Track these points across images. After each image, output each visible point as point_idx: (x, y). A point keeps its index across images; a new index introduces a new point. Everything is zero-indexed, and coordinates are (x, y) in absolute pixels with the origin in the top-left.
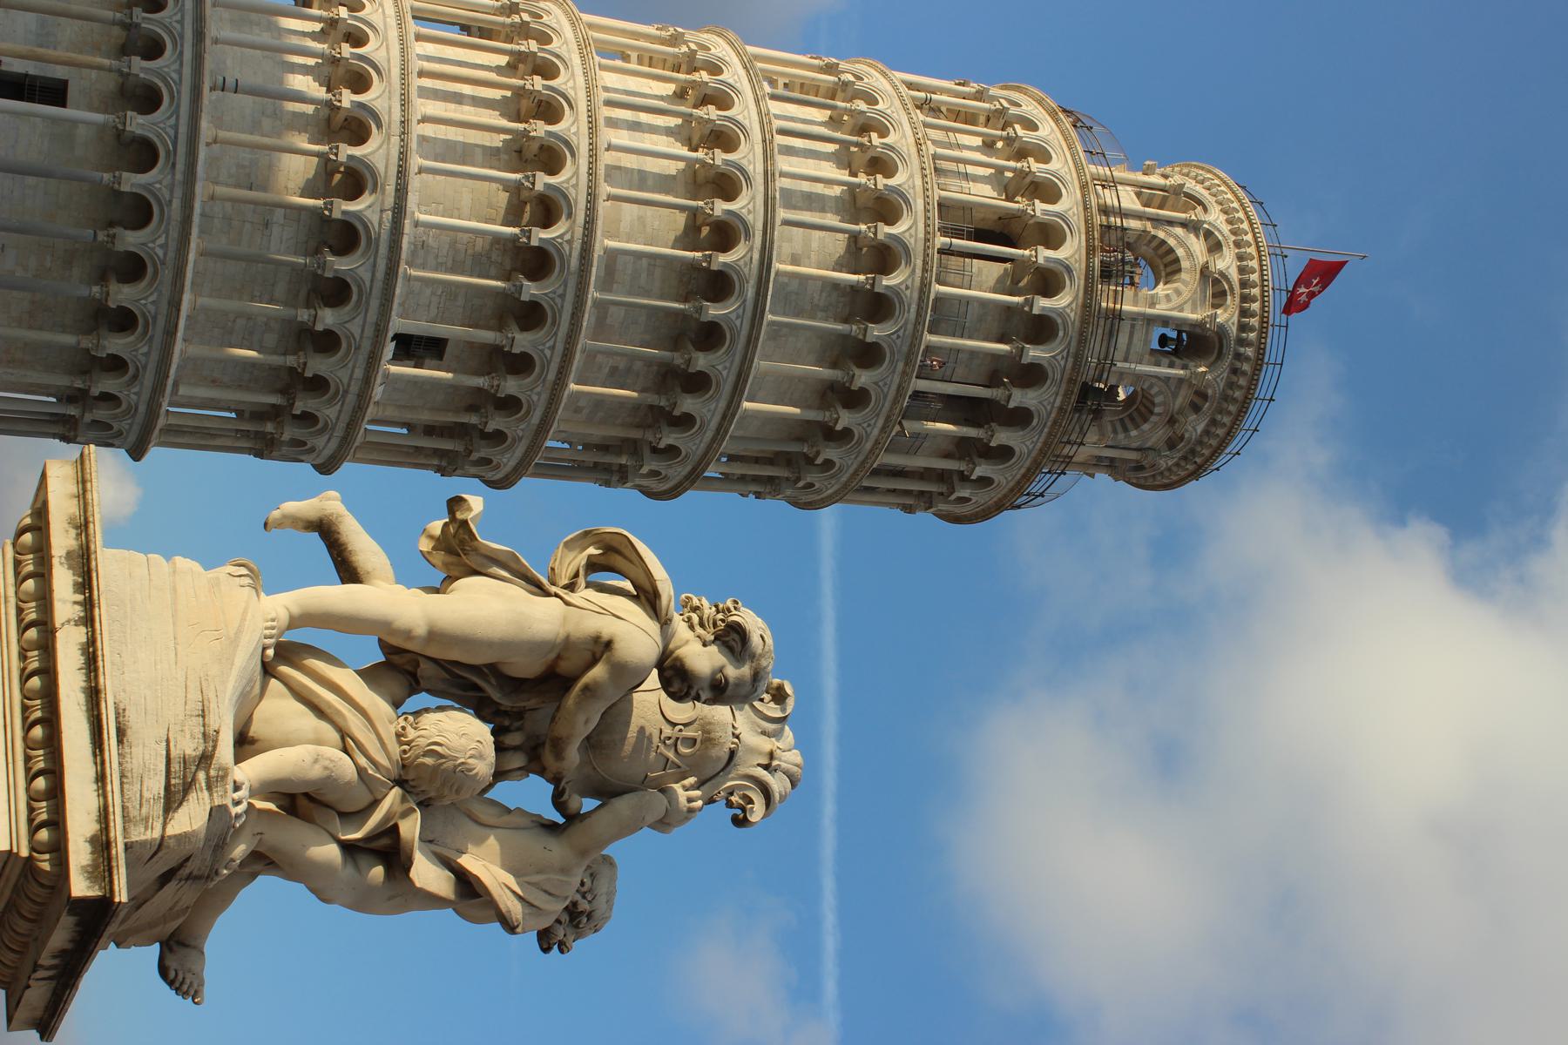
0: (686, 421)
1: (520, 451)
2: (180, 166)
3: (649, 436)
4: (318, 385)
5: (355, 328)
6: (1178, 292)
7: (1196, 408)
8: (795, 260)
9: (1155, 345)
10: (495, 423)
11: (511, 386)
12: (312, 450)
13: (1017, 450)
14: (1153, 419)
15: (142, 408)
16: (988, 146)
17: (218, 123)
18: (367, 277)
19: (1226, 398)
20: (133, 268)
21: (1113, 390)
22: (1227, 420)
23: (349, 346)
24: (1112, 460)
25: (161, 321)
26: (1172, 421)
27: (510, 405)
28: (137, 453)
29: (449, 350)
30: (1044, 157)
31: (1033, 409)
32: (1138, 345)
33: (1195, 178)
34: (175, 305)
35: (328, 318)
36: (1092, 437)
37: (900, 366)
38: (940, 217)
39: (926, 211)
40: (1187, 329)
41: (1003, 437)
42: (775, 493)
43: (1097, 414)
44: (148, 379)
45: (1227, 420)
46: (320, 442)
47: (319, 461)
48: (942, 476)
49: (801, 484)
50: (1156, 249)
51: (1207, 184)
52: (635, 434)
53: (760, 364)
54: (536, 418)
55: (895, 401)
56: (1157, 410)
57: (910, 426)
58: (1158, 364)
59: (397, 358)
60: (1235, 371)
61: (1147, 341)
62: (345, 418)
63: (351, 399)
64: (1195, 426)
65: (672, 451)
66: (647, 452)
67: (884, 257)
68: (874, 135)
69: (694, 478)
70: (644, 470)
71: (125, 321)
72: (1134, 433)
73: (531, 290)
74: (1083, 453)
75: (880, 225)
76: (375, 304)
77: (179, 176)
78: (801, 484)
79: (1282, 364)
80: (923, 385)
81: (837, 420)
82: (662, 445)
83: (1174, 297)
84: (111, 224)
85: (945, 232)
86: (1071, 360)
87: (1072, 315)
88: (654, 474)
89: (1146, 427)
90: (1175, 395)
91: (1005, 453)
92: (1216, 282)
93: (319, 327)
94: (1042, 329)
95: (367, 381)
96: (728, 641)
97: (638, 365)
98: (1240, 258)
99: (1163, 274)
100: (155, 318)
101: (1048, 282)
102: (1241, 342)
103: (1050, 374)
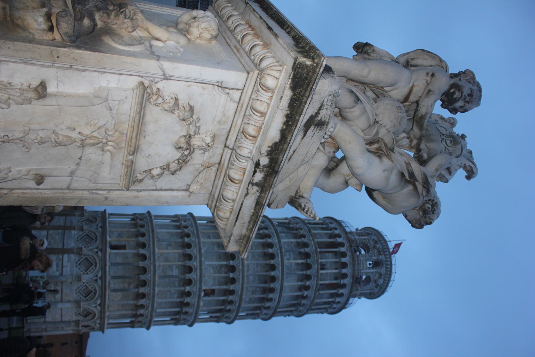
0: (270, 300)
1: (235, 313)
2: (152, 259)
3: (263, 304)
4: (188, 304)
5: (194, 289)
6: (371, 253)
7: (380, 278)
8: (288, 259)
9: (368, 266)
10: (228, 307)
11: (231, 298)
12: (188, 321)
13: (345, 294)
14: (372, 282)
15: (149, 316)
16: (323, 229)
17: (159, 249)
18: (195, 277)
19: (386, 273)
20: (144, 284)
21: (361, 277)
22: (387, 279)
23: (194, 294)
24: (364, 293)
25: (151, 294)
26: (375, 282)
27: (231, 302)
28: (148, 328)
29: (216, 292)
30: (336, 229)
31: (346, 283)
32: (365, 266)
33: (367, 230)
34: (154, 290)
35: (188, 288)
36: (360, 288)
37: (316, 279)
38: (318, 245)
39: (314, 244)
40: (374, 260)
41: (341, 291)
42: (292, 315)
43: (359, 283)
44: (150, 309)
45: (387, 279)
46: (190, 318)
47: (189, 324)
48: (329, 303)
49: (298, 311)
50: (364, 245)
51: (370, 230)
52: (260, 305)
53: (285, 284)
54: (237, 304)
55: (316, 287)
56: (372, 280)
57: (321, 292)
58: (370, 269)
59: (205, 295)
60: (386, 268)
61: (366, 265)
62: (195, 311)
63: (195, 306)
64: (381, 281)
65: (269, 308)
66: (263, 309)
67: (307, 256)
68: (300, 230)
69: (275, 313)
70: (263, 313)
71: (143, 296)
72: (368, 286)
73: (231, 275)
74: (359, 292)
75: (305, 248)
76: (198, 283)
77: (152, 261)
78: (298, 311)
79: (396, 264)
80: (321, 282)
81: (304, 294)
82: (266, 306)
83: (370, 254)
84: (139, 274)
85: (319, 248)
86: (352, 271)
87: (350, 261)
88: (265, 314)
89: (370, 284)
90: (375, 276)
91: (342, 295)
92: (378, 249)
93: (186, 291)
94: (344, 265)
95: (199, 301)
96: (468, 79)
97: (258, 289)
98: (381, 244)
99: (366, 250)
100: (150, 294)
101: (344, 255)
102: (386, 261)
103: (348, 274)
